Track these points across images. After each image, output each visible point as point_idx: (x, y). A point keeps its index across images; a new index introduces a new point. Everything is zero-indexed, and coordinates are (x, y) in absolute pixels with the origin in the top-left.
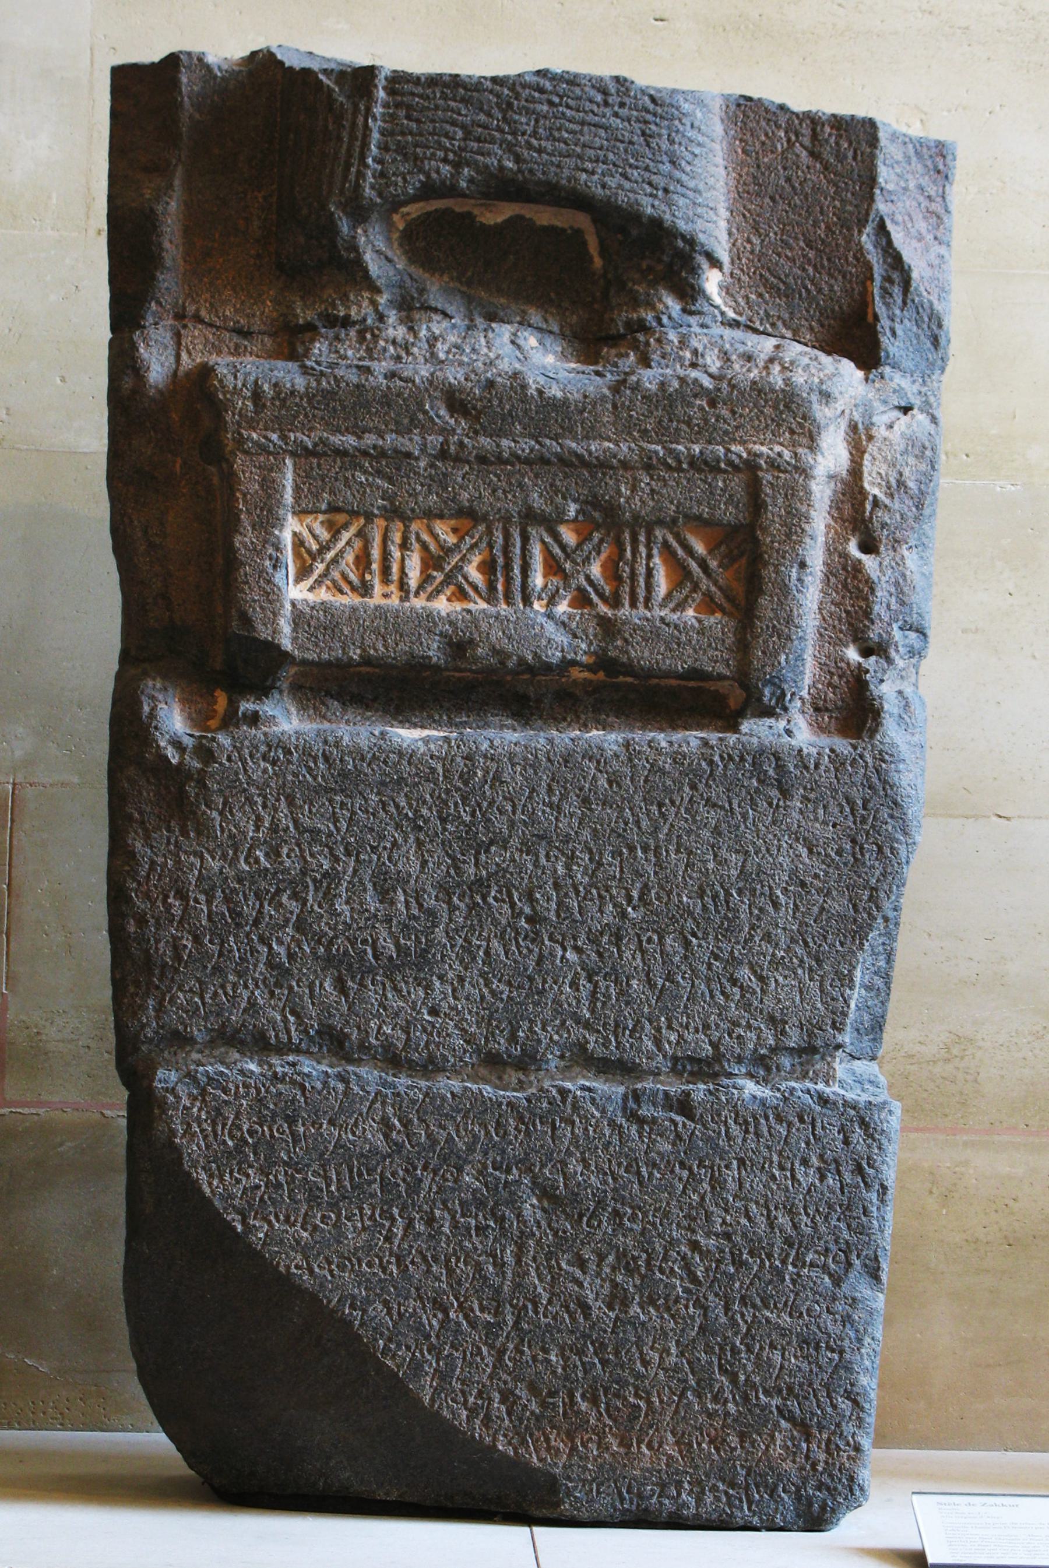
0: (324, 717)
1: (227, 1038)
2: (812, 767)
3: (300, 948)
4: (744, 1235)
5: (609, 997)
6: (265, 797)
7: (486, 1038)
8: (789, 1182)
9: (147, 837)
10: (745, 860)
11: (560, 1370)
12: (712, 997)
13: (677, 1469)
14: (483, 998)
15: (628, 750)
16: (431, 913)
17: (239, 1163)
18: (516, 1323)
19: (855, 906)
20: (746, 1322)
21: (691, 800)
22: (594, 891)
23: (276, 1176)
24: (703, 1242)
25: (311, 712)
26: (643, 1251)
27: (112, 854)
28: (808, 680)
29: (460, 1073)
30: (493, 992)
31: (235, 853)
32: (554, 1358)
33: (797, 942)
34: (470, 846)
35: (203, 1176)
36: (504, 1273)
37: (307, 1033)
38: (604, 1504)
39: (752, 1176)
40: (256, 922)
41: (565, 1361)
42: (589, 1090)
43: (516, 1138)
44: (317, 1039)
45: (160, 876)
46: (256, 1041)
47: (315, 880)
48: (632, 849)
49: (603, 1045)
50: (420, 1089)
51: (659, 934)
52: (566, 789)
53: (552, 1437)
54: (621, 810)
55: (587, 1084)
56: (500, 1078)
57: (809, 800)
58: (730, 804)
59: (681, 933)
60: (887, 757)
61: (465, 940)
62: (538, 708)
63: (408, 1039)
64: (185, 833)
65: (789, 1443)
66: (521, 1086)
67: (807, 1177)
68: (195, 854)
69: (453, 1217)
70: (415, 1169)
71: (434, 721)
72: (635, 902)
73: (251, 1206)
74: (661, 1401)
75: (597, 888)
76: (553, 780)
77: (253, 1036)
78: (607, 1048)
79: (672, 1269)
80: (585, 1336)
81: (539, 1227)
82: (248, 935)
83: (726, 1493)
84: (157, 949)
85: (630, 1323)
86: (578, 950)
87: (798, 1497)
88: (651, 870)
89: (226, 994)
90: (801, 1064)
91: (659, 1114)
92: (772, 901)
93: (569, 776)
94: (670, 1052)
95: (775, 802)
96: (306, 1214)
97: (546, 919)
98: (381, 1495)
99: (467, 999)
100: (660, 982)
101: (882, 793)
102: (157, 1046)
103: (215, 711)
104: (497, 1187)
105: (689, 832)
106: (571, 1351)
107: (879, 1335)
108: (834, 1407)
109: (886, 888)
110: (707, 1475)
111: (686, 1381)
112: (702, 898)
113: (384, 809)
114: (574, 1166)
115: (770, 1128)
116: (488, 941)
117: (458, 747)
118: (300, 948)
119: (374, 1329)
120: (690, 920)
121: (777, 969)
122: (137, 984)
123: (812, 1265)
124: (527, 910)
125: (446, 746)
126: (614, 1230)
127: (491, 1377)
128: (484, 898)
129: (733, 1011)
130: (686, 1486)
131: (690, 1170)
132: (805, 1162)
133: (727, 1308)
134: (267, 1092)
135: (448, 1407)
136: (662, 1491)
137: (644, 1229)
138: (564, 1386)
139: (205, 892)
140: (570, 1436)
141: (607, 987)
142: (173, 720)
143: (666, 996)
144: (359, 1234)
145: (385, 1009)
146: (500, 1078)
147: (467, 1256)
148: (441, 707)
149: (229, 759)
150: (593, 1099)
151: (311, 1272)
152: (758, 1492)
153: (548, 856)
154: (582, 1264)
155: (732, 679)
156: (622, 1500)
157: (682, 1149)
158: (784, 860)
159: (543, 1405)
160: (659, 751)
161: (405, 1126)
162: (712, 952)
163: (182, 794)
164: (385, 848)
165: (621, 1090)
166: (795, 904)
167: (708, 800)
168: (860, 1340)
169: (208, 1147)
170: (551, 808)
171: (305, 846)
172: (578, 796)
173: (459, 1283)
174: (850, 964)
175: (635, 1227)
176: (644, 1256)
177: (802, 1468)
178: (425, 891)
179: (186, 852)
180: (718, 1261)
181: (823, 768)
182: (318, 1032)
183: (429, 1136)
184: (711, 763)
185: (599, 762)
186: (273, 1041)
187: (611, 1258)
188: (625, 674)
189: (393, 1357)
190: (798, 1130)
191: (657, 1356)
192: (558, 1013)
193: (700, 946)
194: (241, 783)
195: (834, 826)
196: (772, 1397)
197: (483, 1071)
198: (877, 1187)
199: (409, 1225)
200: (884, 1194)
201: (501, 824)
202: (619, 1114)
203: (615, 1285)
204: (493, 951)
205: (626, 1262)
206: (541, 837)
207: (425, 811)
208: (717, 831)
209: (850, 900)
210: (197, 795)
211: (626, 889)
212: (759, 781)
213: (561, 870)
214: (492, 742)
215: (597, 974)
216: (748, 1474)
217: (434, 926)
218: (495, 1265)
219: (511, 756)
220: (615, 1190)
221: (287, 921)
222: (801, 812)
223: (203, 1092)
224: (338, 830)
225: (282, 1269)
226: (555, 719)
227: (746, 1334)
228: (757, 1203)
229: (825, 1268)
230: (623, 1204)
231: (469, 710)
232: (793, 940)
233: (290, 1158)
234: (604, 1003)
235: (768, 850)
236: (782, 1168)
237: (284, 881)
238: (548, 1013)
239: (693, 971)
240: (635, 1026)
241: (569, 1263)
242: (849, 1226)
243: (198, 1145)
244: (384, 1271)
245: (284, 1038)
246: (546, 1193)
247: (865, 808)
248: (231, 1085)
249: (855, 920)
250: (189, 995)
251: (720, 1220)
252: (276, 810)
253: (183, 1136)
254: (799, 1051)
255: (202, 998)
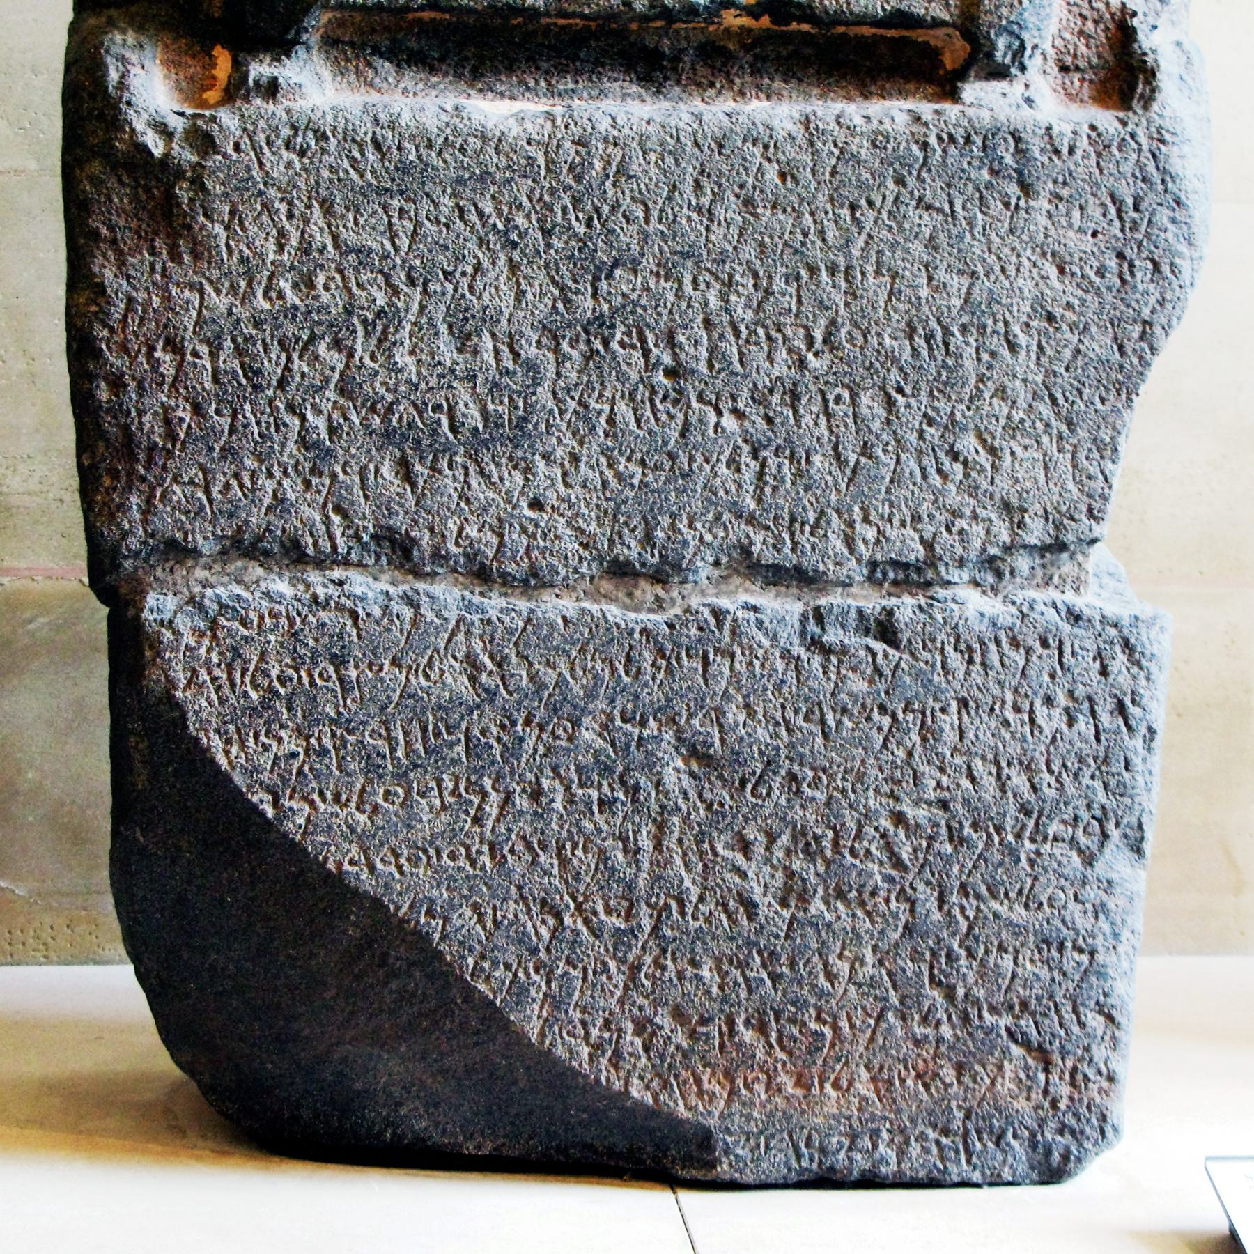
0: (371, 85)
1: (243, 547)
2: (1065, 151)
3: (346, 419)
4: (966, 803)
5: (780, 479)
6: (290, 203)
7: (611, 540)
8: (1027, 728)
9: (121, 263)
10: (972, 285)
11: (715, 990)
12: (924, 477)
13: (873, 1114)
14: (605, 484)
15: (807, 129)
16: (532, 367)
17: (268, 723)
18: (656, 929)
19: (1121, 347)
20: (967, 918)
21: (897, 199)
22: (761, 331)
23: (319, 739)
24: (910, 812)
25: (353, 77)
26: (828, 827)
27: (73, 285)
28: (1052, 28)
29: (574, 589)
30: (619, 476)
31: (250, 284)
32: (706, 973)
33: (1042, 399)
34: (585, 269)
35: (217, 742)
36: (637, 862)
37: (359, 538)
38: (776, 1162)
39: (977, 723)
40: (282, 384)
41: (723, 978)
42: (755, 609)
43: (654, 679)
44: (373, 547)
45: (142, 319)
46: (286, 551)
47: (365, 322)
48: (813, 270)
49: (774, 546)
50: (519, 614)
51: (851, 389)
52: (720, 186)
53: (705, 1078)
54: (798, 215)
55: (753, 600)
56: (630, 595)
57: (1061, 199)
58: (951, 204)
59: (883, 388)
60: (1167, 137)
61: (580, 403)
62: (674, 69)
63: (501, 544)
64: (175, 256)
65: (1022, 1075)
66: (659, 605)
67: (1051, 720)
68: (192, 286)
69: (568, 788)
70: (514, 723)
71: (528, 89)
72: (818, 345)
73: (285, 781)
74: (852, 1026)
75: (765, 327)
76: (702, 172)
77: (282, 545)
78: (779, 551)
79: (868, 851)
80: (749, 944)
81: (686, 798)
82: (271, 402)
83: (938, 1143)
84: (140, 423)
85: (811, 924)
86: (739, 414)
87: (1034, 1145)
88: (840, 299)
89: (241, 486)
90: (1044, 566)
91: (854, 641)
92: (1008, 342)
93: (725, 168)
94: (867, 555)
95: (1013, 201)
96: (363, 790)
97: (693, 372)
98: (469, 1148)
99: (584, 487)
100: (852, 458)
101: (1160, 188)
102: (146, 561)
103: (214, 78)
104: (628, 747)
105: (894, 246)
106: (731, 962)
107: (1139, 927)
108: (1082, 1025)
109: (1164, 321)
110: (912, 1121)
111: (886, 999)
112: (911, 338)
113: (462, 218)
114: (735, 714)
115: (1002, 655)
116: (613, 402)
117: (566, 127)
118: (346, 419)
119: (461, 943)
120: (894, 371)
121: (1014, 437)
122: (114, 474)
123: (1055, 839)
124: (667, 360)
125: (549, 125)
126: (789, 801)
127: (621, 1002)
128: (606, 343)
129: (953, 497)
130: (885, 1135)
131: (894, 717)
132: (1049, 701)
133: (941, 901)
134: (304, 622)
135: (563, 1044)
136: (853, 1142)
137: (830, 798)
138: (722, 1011)
139: (208, 342)
140: (729, 1075)
141: (779, 466)
142: (152, 91)
143: (860, 478)
144: (438, 814)
145: (468, 502)
146: (630, 595)
147: (587, 839)
148: (538, 68)
149: (237, 148)
150: (760, 624)
151: (372, 868)
152: (980, 1139)
153: (695, 282)
154: (745, 847)
155: (954, 25)
156: (799, 1156)
157: (882, 687)
158: (1026, 285)
159: (693, 1035)
160: (851, 130)
161: (499, 665)
162: (925, 415)
163: (170, 200)
164: (464, 274)
165: (797, 608)
166: (1040, 347)
167: (920, 200)
168: (1116, 935)
169: (222, 702)
170: (700, 212)
171: (350, 273)
172: (737, 196)
173: (577, 877)
174: (1114, 428)
175: (817, 794)
176: (830, 834)
177: (1039, 1107)
178: (522, 335)
179: (178, 284)
180: (931, 839)
181: (1079, 152)
182: (374, 537)
183: (532, 678)
184: (925, 146)
185: (766, 147)
186: (310, 551)
187: (785, 839)
188: (800, 20)
189: (488, 979)
190: (1040, 657)
191: (847, 966)
192: (712, 503)
193: (908, 406)
194: (255, 184)
195: (1094, 234)
196: (1000, 1015)
197: (606, 586)
198: (1144, 731)
199: (508, 799)
200: (1152, 739)
201: (628, 237)
202: (796, 641)
203: (790, 874)
204: (618, 419)
205: (807, 845)
206: (686, 256)
207: (520, 220)
208: (932, 244)
209: (1116, 339)
210: (191, 200)
211: (806, 328)
212: (993, 172)
213: (714, 303)
214: (614, 119)
215: (765, 447)
216: (967, 1117)
217: (536, 383)
218: (625, 851)
219: (643, 139)
220: (791, 746)
221: (327, 380)
222: (1049, 215)
223: (214, 625)
224: (397, 249)
225: (331, 866)
226: (699, 85)
227: (968, 934)
228: (983, 758)
229: (1073, 841)
230: (801, 764)
231: (578, 72)
232: (1035, 396)
233: (339, 713)
234: (775, 489)
235: (1003, 270)
236: (1017, 709)
237: (320, 323)
238: (697, 505)
239: (898, 441)
240: (818, 520)
241: (727, 846)
242: (1106, 786)
243: (208, 699)
244: (473, 863)
245: (326, 545)
246: (696, 752)
247: (1136, 208)
248: (252, 615)
249: (1121, 367)
250: (188, 490)
251: (934, 783)
252: (306, 221)
253: (188, 686)
254: (1044, 549)
255: (208, 492)
